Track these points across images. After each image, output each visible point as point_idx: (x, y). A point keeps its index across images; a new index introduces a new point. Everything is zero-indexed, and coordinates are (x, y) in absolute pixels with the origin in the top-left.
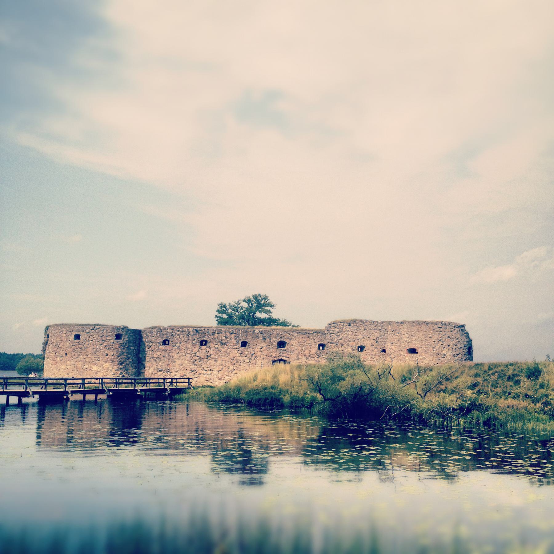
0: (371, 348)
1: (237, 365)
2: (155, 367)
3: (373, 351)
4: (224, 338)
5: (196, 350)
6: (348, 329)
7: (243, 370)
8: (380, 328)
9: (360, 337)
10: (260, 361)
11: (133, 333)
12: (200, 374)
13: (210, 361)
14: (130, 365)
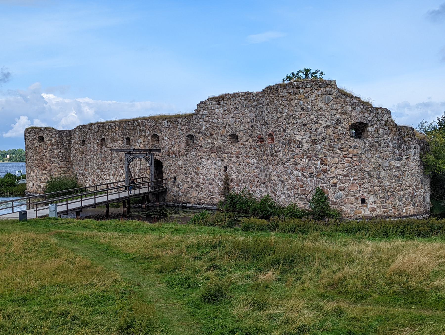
3: (247, 141)
6: (217, 110)
8: (255, 103)
9: (232, 120)
13: (108, 164)
14: (55, 170)
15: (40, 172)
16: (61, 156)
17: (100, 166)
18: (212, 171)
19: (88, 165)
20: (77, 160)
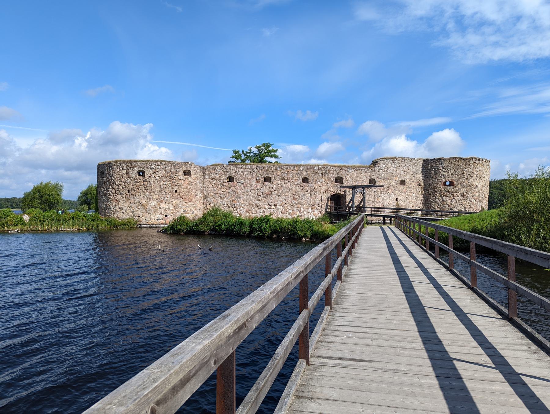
0: (410, 183)
1: (299, 199)
2: (221, 203)
4: (286, 175)
5: (259, 186)
8: (416, 164)
9: (402, 172)
10: (320, 196)
13: (274, 196)
17: (260, 199)
18: (388, 201)
19: (240, 198)
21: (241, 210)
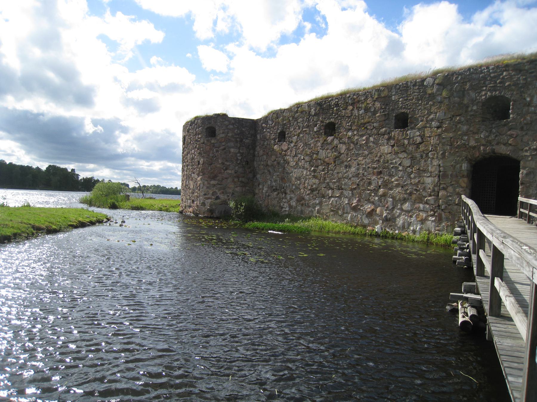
7: (397, 186)
11: (233, 124)
12: (323, 196)
14: (230, 180)
15: (206, 182)
16: (240, 158)
20: (267, 165)
21: (291, 198)
